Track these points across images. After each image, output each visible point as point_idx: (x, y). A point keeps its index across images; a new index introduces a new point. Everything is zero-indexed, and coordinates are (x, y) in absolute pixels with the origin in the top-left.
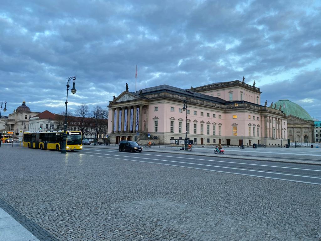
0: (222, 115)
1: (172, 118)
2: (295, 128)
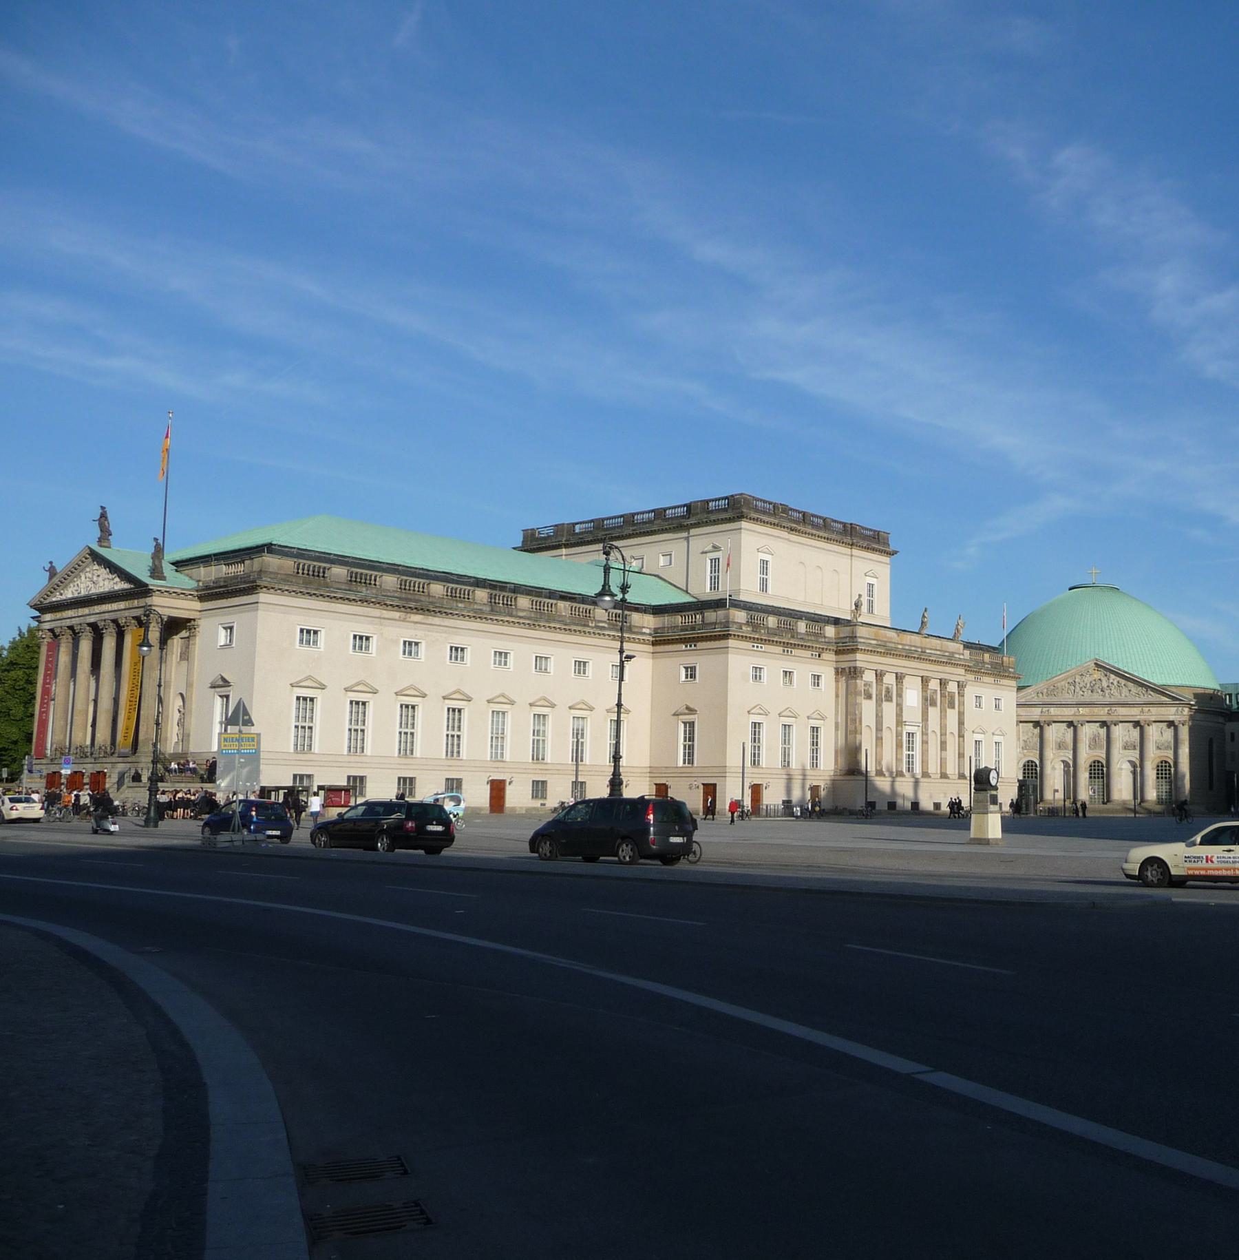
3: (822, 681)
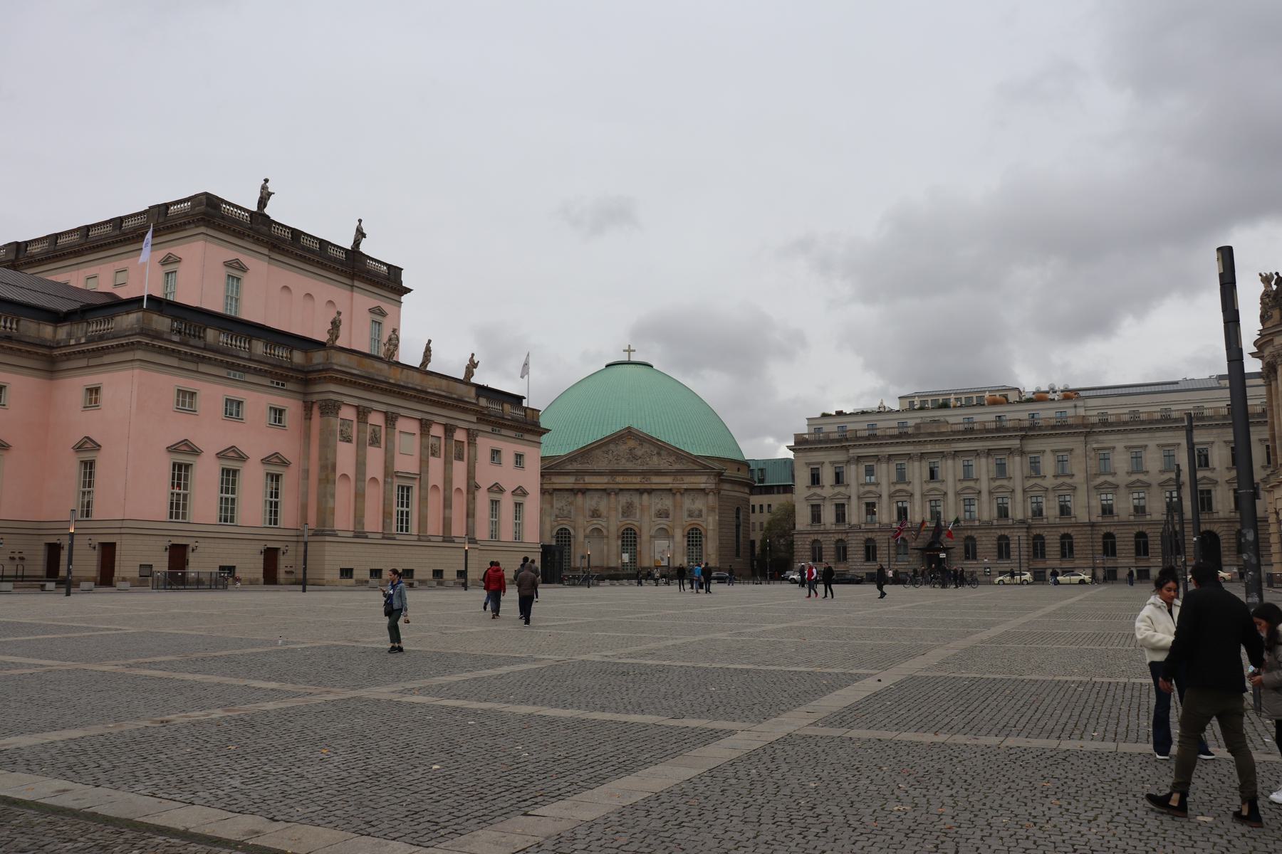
2: (650, 492)
3: (287, 418)
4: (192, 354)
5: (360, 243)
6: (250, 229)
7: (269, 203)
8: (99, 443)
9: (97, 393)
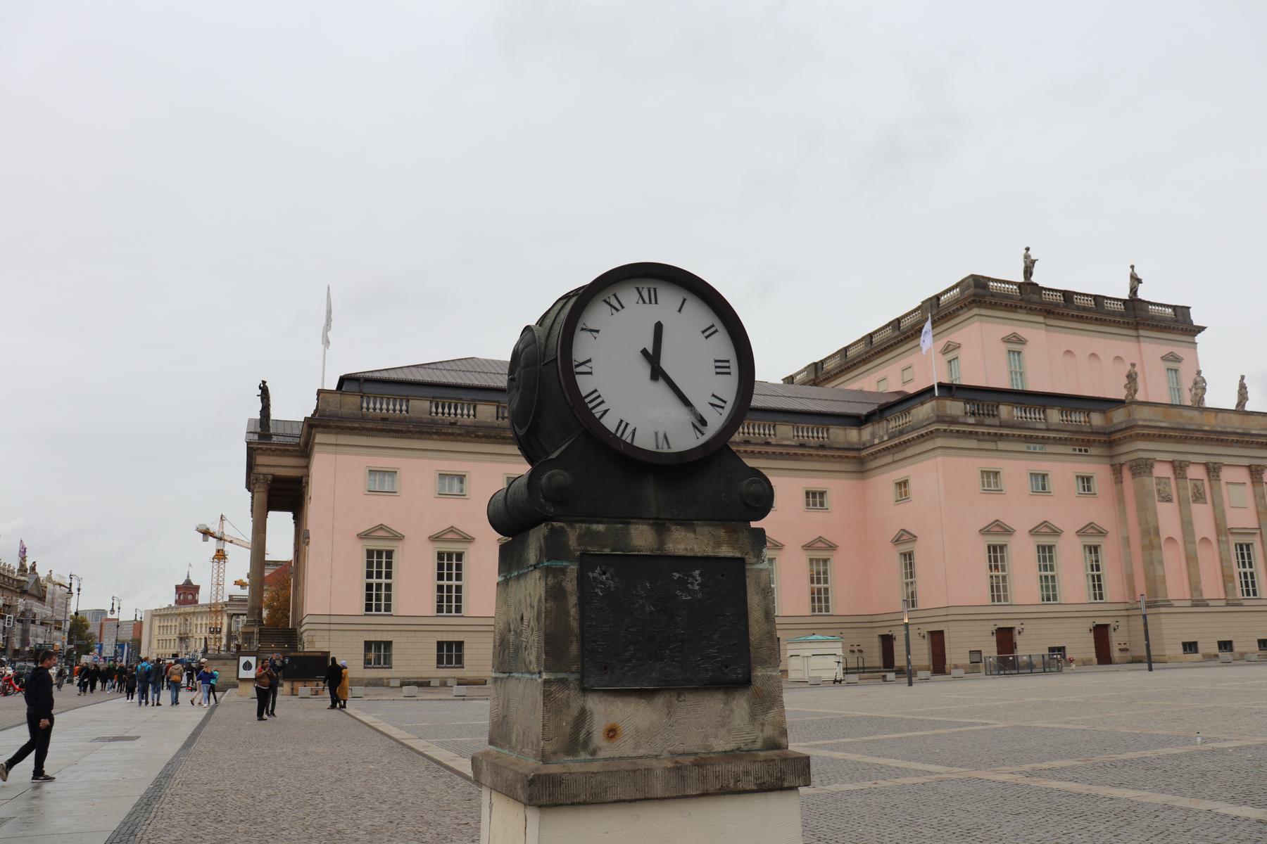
0: (837, 487)
1: (1045, 530)
3: (1095, 485)
4: (989, 433)
5: (1136, 291)
6: (1021, 300)
7: (1035, 270)
8: (915, 534)
9: (905, 487)
